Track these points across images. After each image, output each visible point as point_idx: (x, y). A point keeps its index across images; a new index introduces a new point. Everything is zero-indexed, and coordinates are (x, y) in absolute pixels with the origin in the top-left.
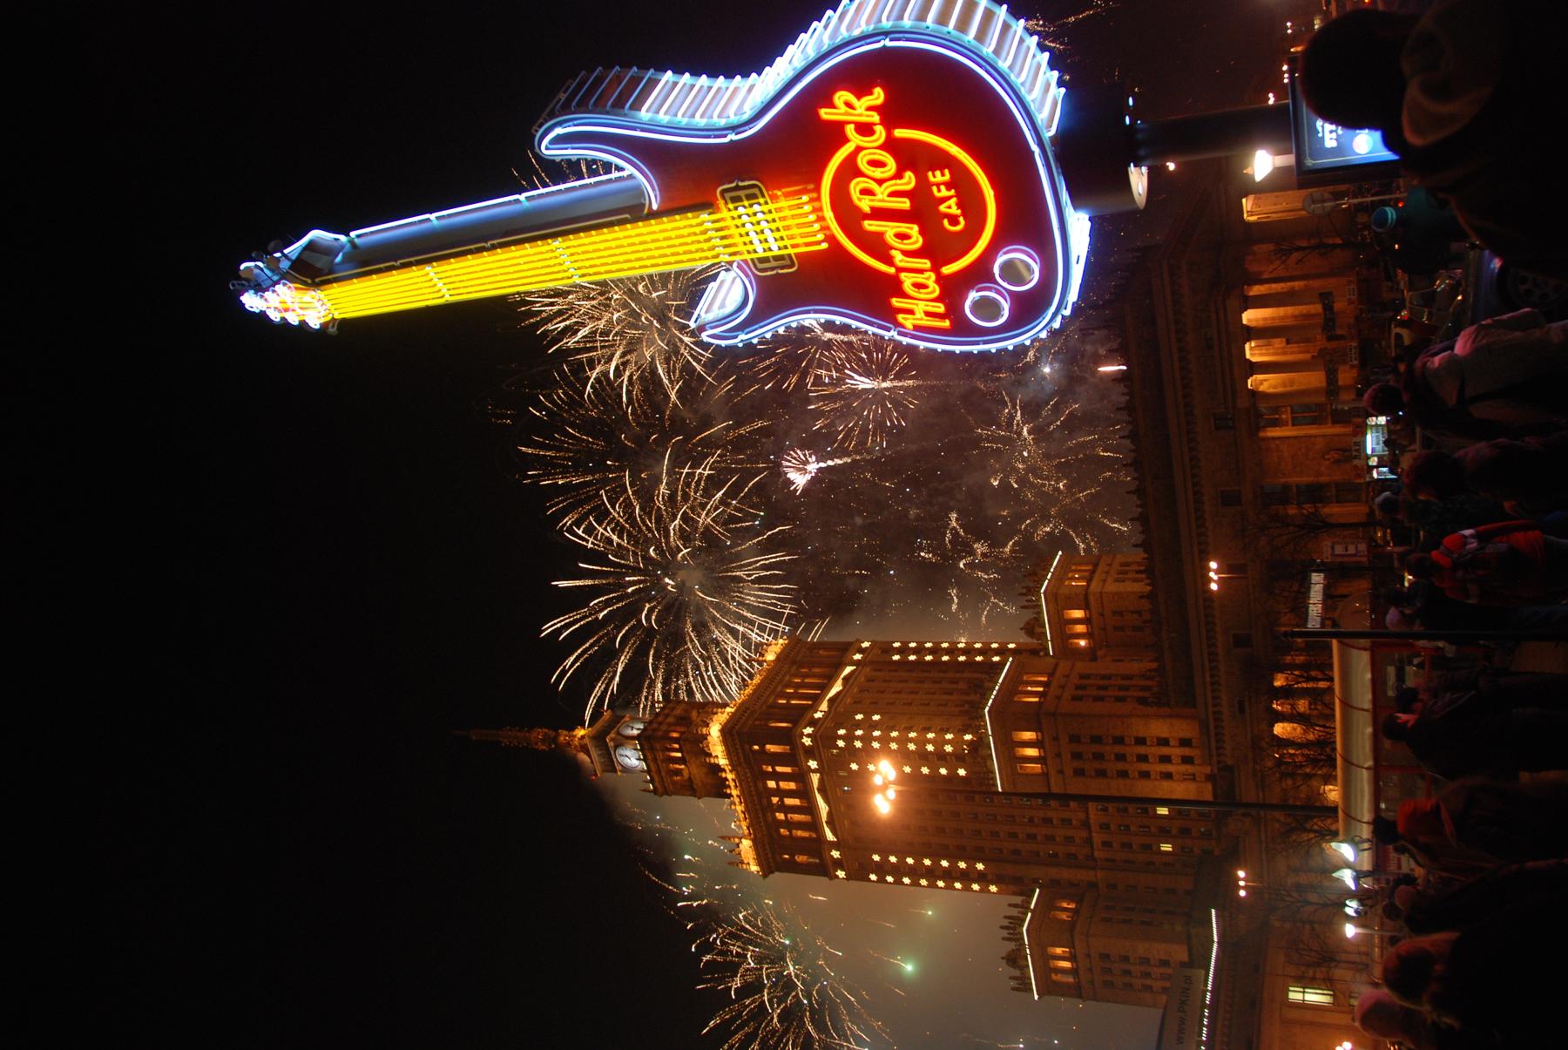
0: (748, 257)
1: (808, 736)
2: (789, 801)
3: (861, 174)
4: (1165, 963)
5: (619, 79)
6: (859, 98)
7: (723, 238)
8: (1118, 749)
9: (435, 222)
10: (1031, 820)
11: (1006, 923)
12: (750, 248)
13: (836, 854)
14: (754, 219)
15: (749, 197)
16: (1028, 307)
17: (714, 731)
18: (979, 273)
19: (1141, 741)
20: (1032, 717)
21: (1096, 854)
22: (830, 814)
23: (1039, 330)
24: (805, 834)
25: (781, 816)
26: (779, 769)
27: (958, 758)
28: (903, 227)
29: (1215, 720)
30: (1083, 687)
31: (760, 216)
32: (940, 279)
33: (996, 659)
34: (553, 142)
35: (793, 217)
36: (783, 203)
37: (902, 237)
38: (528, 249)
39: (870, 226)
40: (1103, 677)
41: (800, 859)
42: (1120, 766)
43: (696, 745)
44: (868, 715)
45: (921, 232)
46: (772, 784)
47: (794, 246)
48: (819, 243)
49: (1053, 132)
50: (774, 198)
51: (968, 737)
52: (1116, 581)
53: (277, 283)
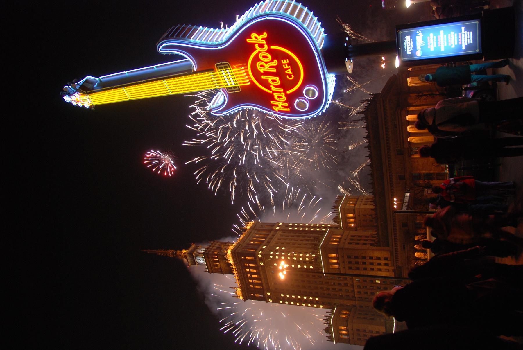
0: (225, 87)
1: (260, 254)
2: (253, 276)
3: (260, 60)
5: (184, 29)
6: (259, 36)
7: (217, 80)
8: (364, 260)
9: (127, 74)
10: (334, 283)
11: (325, 318)
12: (226, 84)
14: (227, 75)
15: (226, 67)
16: (315, 104)
17: (229, 252)
19: (371, 258)
20: (335, 250)
21: (356, 295)
23: (318, 112)
24: (259, 287)
25: (251, 281)
26: (250, 265)
27: (310, 263)
28: (274, 78)
29: (396, 251)
30: (352, 240)
31: (229, 74)
32: (286, 95)
33: (324, 230)
34: (163, 48)
35: (239, 74)
36: (236, 69)
39: (263, 77)
40: (359, 236)
41: (257, 295)
42: (364, 266)
43: (223, 257)
44: (281, 247)
45: (280, 80)
46: (248, 270)
47: (240, 83)
48: (247, 83)
49: (321, 47)
50: (233, 68)
51: (314, 256)
52: (364, 204)
53: (75, 93)
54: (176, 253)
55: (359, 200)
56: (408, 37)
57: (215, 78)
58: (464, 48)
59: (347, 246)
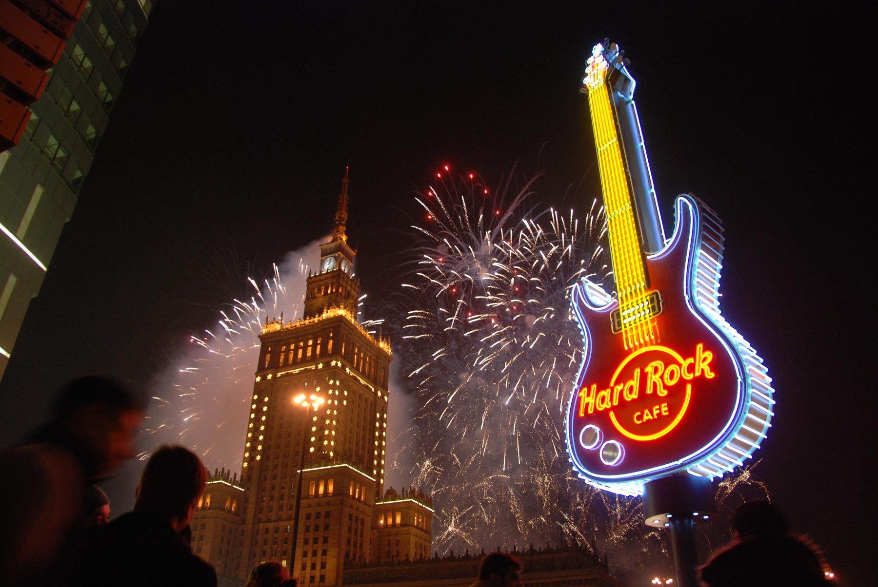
0: (620, 307)
1: (337, 364)
2: (300, 352)
3: (666, 366)
5: (718, 239)
7: (631, 294)
8: (321, 540)
9: (640, 145)
10: (283, 488)
11: (226, 471)
12: (625, 308)
13: (270, 377)
14: (641, 310)
15: (653, 308)
16: (591, 461)
17: (341, 312)
19: (325, 553)
20: (341, 491)
21: (261, 525)
23: (577, 466)
25: (292, 347)
26: (319, 347)
27: (320, 448)
28: (636, 390)
30: (357, 521)
31: (643, 313)
32: (607, 411)
33: (375, 472)
34: (685, 204)
35: (643, 332)
36: (650, 326)
37: (631, 390)
38: (625, 191)
39: (637, 372)
41: (268, 356)
42: (311, 540)
43: (333, 302)
44: (347, 398)
45: (633, 400)
46: (310, 343)
47: (626, 332)
49: (690, 472)
50: (652, 321)
51: (331, 454)
52: (416, 543)
53: (608, 62)
54: (340, 224)
55: (423, 533)
57: (635, 291)
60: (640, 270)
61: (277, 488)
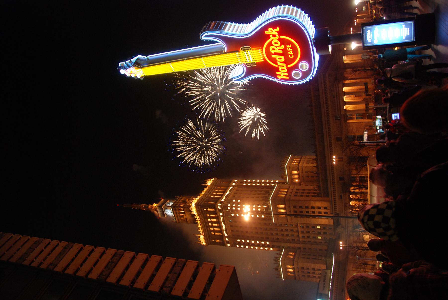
0: (245, 63)
2: (214, 225)
3: (272, 45)
4: (319, 270)
10: (282, 230)
11: (275, 259)
13: (227, 239)
16: (305, 74)
17: (193, 205)
18: (296, 67)
19: (313, 208)
20: (283, 201)
21: (300, 240)
22: (226, 228)
25: (212, 229)
26: (211, 215)
27: (262, 213)
32: (287, 68)
33: (273, 185)
36: (255, 51)
39: (273, 56)
40: (303, 190)
43: (188, 209)
45: (284, 58)
46: (209, 220)
50: (253, 50)
51: (265, 207)
54: (148, 207)
56: (369, 31)
58: (404, 38)
59: (293, 198)
60: (231, 54)
61: (283, 233)
